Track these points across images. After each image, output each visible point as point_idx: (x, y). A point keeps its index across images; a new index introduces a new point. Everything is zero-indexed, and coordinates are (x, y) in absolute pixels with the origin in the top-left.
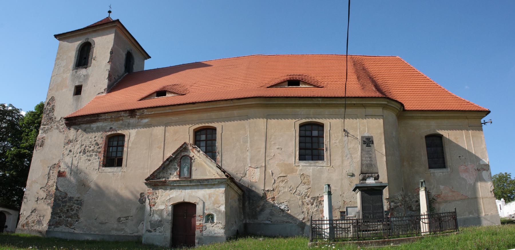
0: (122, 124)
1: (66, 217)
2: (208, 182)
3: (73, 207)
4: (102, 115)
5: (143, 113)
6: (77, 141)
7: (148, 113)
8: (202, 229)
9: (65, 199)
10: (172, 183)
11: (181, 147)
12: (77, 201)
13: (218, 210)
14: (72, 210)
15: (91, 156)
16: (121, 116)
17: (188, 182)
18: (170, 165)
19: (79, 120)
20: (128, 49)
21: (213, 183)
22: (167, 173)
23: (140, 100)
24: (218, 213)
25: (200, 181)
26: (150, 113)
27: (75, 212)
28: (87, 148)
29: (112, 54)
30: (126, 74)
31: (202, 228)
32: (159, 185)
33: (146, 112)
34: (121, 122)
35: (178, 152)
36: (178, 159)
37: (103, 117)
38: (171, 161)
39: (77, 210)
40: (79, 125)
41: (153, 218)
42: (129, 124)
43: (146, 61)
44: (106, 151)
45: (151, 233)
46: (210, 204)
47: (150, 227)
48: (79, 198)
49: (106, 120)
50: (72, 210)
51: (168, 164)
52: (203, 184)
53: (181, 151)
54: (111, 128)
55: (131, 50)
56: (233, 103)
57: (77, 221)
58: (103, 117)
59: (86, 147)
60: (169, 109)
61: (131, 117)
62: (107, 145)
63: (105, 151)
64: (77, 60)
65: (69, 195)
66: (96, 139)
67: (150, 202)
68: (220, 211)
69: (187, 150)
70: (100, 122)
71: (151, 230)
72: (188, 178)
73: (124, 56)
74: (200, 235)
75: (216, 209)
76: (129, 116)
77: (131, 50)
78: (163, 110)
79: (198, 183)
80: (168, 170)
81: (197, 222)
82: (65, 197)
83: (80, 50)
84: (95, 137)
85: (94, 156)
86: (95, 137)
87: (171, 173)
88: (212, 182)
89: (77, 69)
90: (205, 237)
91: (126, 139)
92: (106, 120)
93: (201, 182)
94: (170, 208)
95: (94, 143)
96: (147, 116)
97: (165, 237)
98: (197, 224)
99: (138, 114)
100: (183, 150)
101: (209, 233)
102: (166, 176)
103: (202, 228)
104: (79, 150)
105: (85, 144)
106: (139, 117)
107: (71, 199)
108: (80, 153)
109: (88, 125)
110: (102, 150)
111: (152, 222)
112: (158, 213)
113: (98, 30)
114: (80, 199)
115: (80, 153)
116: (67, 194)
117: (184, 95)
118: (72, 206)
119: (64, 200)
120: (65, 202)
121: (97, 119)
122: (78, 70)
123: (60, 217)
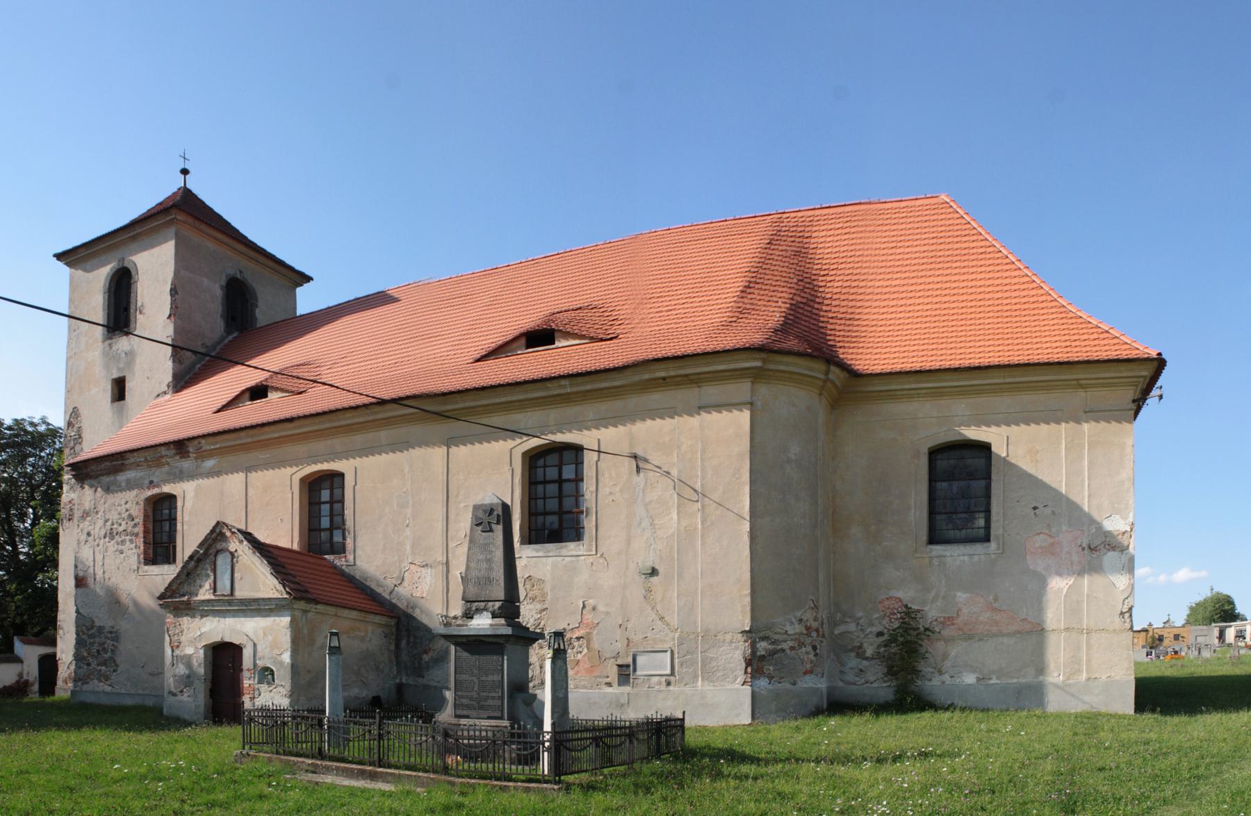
0: (169, 473)
1: (98, 665)
2: (259, 605)
3: (106, 646)
4: (128, 455)
5: (201, 448)
6: (97, 513)
7: (208, 448)
9: (93, 631)
12: (111, 632)
14: (105, 650)
15: (123, 542)
16: (162, 457)
19: (93, 468)
27: (109, 654)
28: (115, 526)
29: (176, 296)
33: (206, 445)
34: (166, 468)
37: (132, 460)
39: (112, 651)
40: (97, 477)
42: (181, 472)
44: (151, 532)
48: (113, 627)
49: (138, 465)
50: (105, 650)
54: (151, 482)
57: (114, 671)
58: (132, 460)
59: (113, 524)
61: (181, 458)
62: (151, 517)
63: (146, 532)
64: (108, 314)
65: (98, 623)
66: (128, 506)
68: (281, 663)
70: (129, 469)
75: (276, 658)
76: (177, 454)
82: (92, 627)
83: (113, 290)
84: (126, 503)
85: (128, 543)
86: (126, 503)
89: (111, 338)
91: (179, 504)
92: (139, 466)
95: (125, 515)
96: (210, 454)
99: (191, 450)
104: (103, 533)
105: (111, 517)
106: (195, 455)
107: (101, 629)
108: (105, 537)
109: (111, 478)
110: (140, 529)
114: (115, 630)
115: (105, 537)
116: (93, 622)
118: (104, 643)
119: (90, 632)
120: (92, 636)
121: (123, 464)
122: (113, 340)
123: (89, 665)
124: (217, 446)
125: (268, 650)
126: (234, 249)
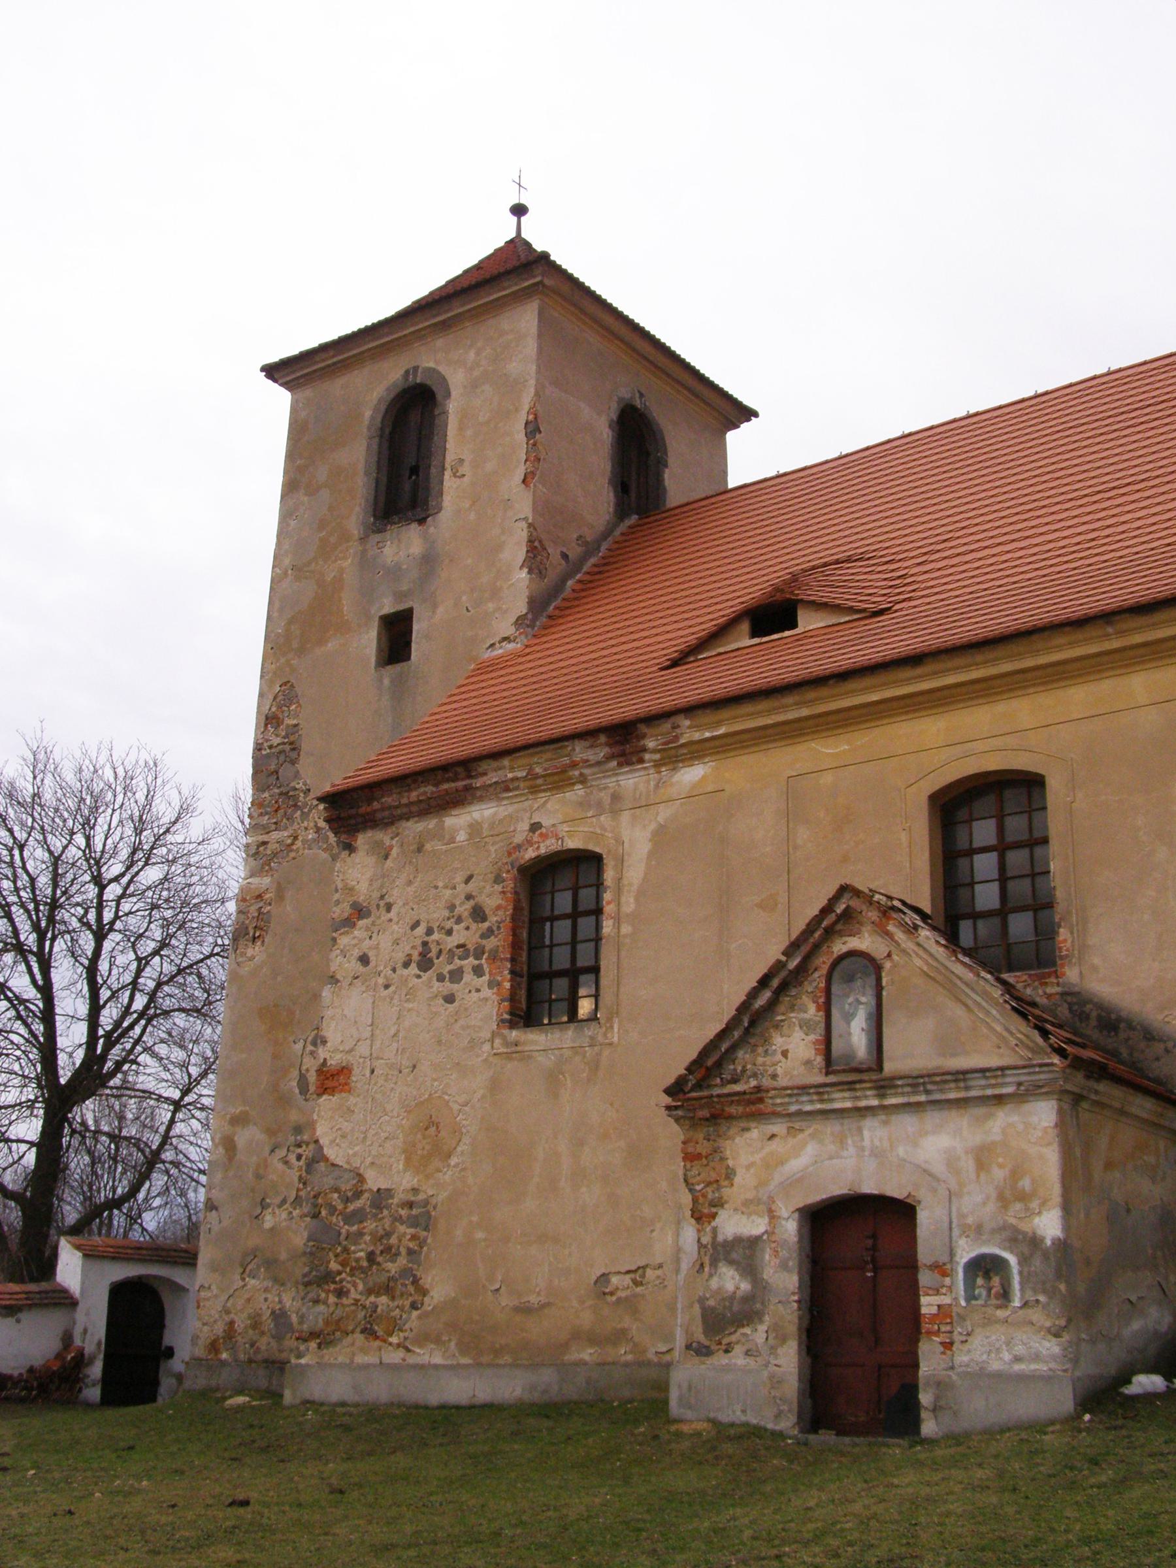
0: (583, 804)
1: (369, 1292)
3: (393, 1240)
4: (484, 766)
5: (677, 738)
6: (389, 908)
7: (697, 736)
8: (951, 1332)
9: (358, 1204)
10: (794, 1099)
11: (826, 911)
12: (410, 1205)
13: (1025, 1234)
14: (390, 1252)
15: (456, 976)
16: (574, 765)
17: (869, 1093)
18: (781, 1008)
19: (388, 800)
20: (625, 393)
21: (989, 1092)
22: (766, 1051)
23: (675, 663)
24: (1026, 1251)
25: (924, 1084)
26: (707, 735)
27: (402, 1261)
28: (436, 936)
29: (538, 436)
30: (623, 527)
31: (948, 1328)
32: (730, 1117)
33: (690, 732)
34: (579, 791)
35: (811, 940)
36: (816, 975)
37: (492, 778)
38: (783, 987)
39: (410, 1252)
40: (392, 823)
41: (714, 1283)
42: (616, 797)
43: (731, 436)
44: (525, 947)
45: (710, 1361)
46: (984, 1204)
47: (700, 1330)
48: (415, 1191)
49: (506, 787)
50: (390, 1252)
51: (772, 1004)
52: (943, 1097)
53: (830, 933)
54: (535, 827)
55: (641, 395)
56: (1122, 633)
57: (414, 1306)
58: (492, 778)
59: (430, 931)
60: (796, 704)
61: (620, 765)
62: (526, 913)
63: (515, 945)
65: (374, 1181)
66: (471, 885)
67: (695, 1200)
68: (1035, 1241)
69: (857, 926)
70: (481, 799)
71: (707, 1343)
72: (869, 1070)
73: (606, 435)
74: (943, 1366)
76: (610, 757)
77: (641, 395)
78: (770, 712)
79: (915, 1093)
80: (774, 1035)
81: (924, 1300)
82: (358, 1194)
83: (387, 431)
84: (468, 880)
85: (468, 977)
86: (468, 880)
87: (787, 1051)
88: (984, 1087)
90: (965, 1375)
91: (609, 875)
92: (507, 789)
93: (929, 1087)
94: (790, 1228)
95: (464, 909)
96: (697, 752)
97: (772, 1377)
98: (924, 1310)
99: (651, 744)
100: (839, 927)
101: (985, 1357)
102: (764, 1064)
103: (948, 1328)
104: (400, 957)
105: (423, 917)
106: (657, 756)
107: (381, 1198)
108: (406, 965)
109: (431, 823)
110: (499, 942)
111: (711, 1303)
112: (734, 1256)
113: (458, 318)
114: (422, 1196)
115: (406, 965)
116: (361, 1179)
117: (882, 612)
118: (388, 1235)
119: (351, 1207)
120: (358, 1217)
121: (467, 788)
123: (341, 1293)
124: (722, 731)
125: (991, 1207)
126: (634, 350)
